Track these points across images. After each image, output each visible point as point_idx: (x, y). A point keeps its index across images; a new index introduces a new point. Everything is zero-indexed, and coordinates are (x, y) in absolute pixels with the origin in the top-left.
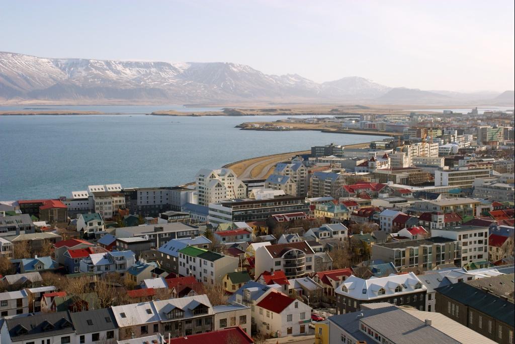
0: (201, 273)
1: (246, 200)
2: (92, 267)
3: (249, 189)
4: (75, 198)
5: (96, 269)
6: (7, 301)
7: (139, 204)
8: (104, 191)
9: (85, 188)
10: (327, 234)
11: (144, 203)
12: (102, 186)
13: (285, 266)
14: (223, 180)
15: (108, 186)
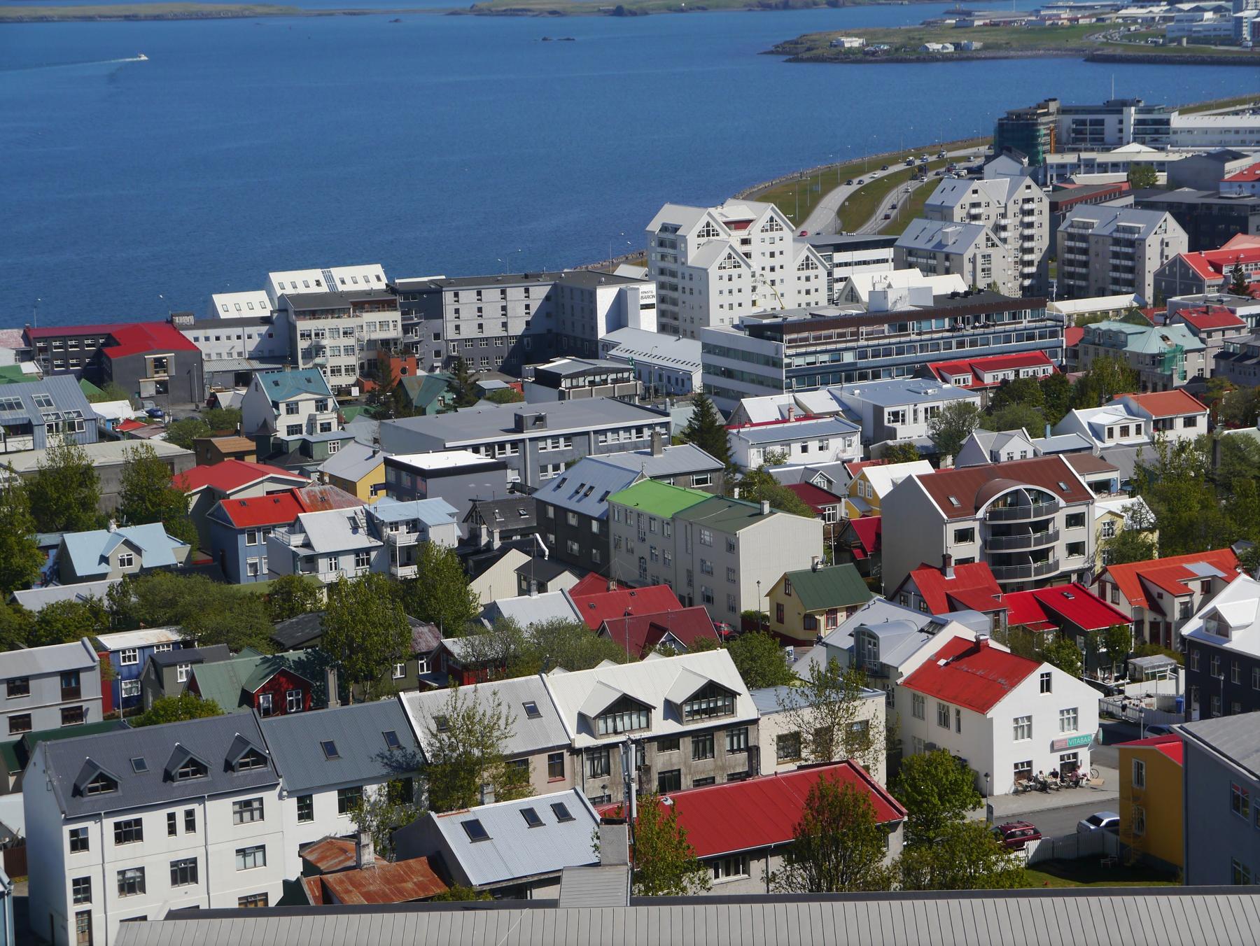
0: (690, 573)
1: (832, 312)
2: (311, 561)
3: (838, 272)
4: (223, 315)
5: (323, 564)
6: (26, 679)
7: (450, 334)
8: (324, 289)
9: (261, 283)
10: (1132, 430)
11: (469, 331)
12: (317, 274)
13: (986, 544)
14: (745, 242)
15: (337, 272)
